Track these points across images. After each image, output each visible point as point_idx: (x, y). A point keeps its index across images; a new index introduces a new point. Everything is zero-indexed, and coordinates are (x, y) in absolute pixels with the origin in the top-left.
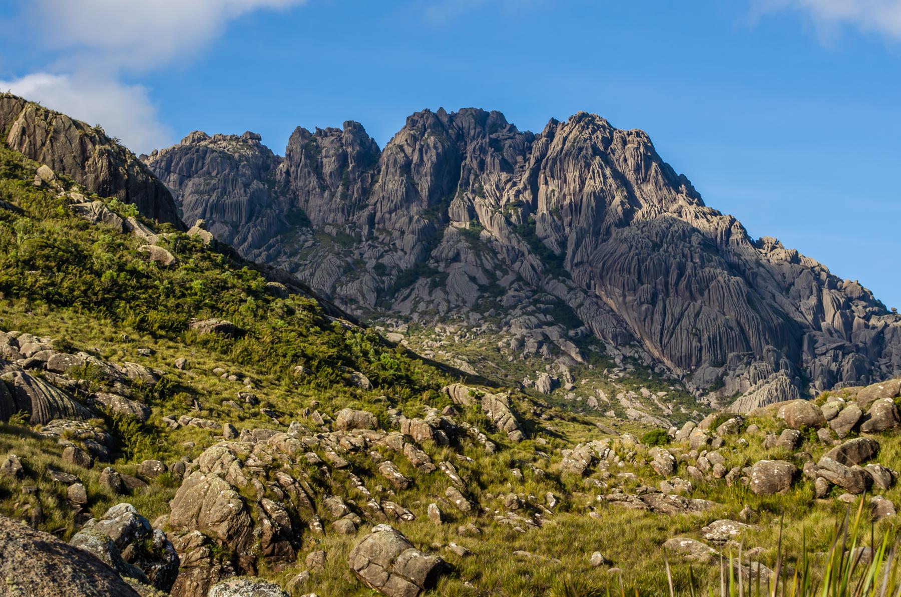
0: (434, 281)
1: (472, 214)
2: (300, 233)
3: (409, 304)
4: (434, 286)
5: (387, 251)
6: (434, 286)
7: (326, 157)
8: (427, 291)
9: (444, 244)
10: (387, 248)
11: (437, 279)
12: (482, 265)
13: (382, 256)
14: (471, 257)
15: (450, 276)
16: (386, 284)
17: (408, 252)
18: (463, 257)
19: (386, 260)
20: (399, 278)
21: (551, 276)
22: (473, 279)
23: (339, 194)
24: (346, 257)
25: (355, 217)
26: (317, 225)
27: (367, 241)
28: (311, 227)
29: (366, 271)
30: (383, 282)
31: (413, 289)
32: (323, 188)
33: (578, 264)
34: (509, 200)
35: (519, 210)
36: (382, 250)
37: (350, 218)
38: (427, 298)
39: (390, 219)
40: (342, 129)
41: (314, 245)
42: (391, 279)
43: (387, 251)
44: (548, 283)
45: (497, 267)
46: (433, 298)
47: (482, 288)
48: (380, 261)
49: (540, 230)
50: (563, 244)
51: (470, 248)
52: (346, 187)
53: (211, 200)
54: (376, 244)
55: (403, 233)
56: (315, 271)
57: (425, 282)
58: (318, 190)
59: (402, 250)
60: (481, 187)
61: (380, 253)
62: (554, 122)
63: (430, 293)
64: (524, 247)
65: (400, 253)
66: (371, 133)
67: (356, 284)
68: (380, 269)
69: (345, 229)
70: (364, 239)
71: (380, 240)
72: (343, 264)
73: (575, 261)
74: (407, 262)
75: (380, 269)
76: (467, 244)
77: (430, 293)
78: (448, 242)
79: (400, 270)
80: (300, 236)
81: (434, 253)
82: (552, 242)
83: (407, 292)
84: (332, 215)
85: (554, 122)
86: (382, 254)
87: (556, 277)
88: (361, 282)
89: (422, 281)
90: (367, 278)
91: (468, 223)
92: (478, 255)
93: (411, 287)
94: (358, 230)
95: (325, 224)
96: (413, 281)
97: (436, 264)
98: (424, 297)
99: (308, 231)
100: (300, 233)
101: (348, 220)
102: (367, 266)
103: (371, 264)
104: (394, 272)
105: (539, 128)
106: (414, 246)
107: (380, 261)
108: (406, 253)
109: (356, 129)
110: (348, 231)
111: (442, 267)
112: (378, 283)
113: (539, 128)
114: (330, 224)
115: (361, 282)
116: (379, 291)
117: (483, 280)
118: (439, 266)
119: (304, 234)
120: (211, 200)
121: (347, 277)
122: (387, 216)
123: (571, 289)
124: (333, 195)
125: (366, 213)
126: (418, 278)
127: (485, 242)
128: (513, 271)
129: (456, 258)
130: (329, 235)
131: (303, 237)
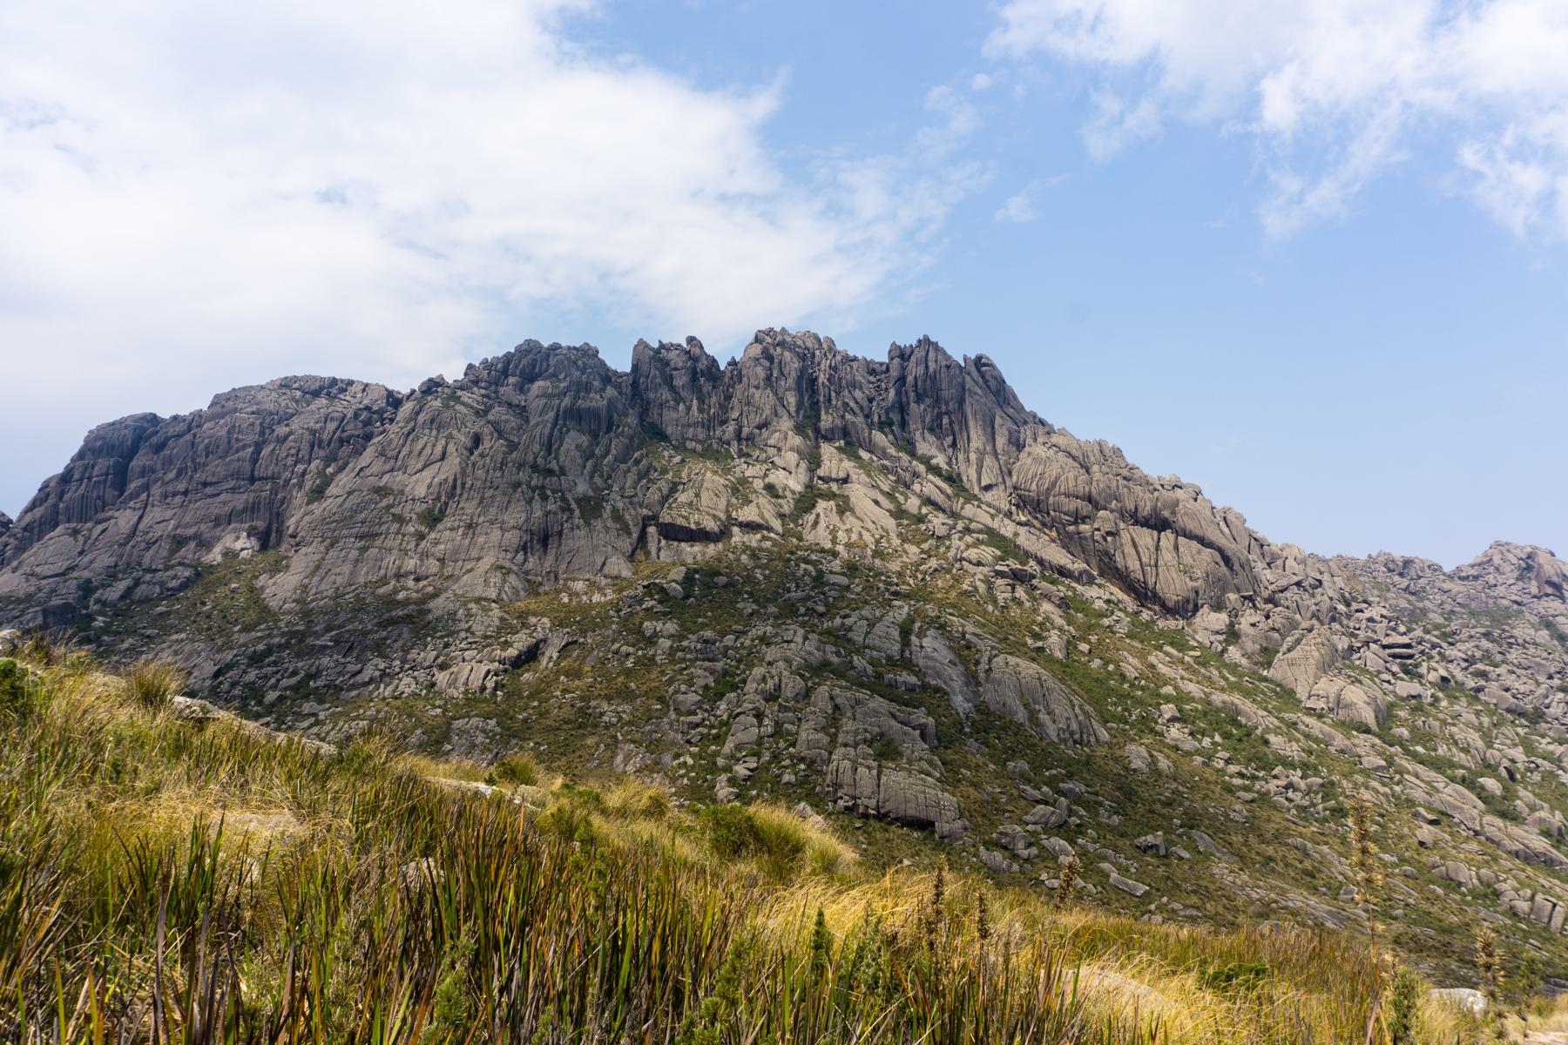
5: (768, 470)
7: (675, 369)
9: (827, 462)
12: (877, 487)
13: (766, 475)
14: (864, 478)
17: (793, 470)
18: (854, 477)
20: (797, 501)
21: (962, 500)
22: (876, 502)
23: (695, 408)
29: (756, 492)
30: (781, 506)
31: (818, 515)
33: (988, 488)
39: (760, 435)
40: (684, 345)
44: (962, 508)
45: (893, 489)
48: (767, 480)
53: (563, 405)
55: (779, 450)
58: (672, 403)
73: (983, 484)
79: (793, 492)
83: (812, 518)
84: (691, 429)
87: (968, 501)
92: (869, 476)
93: (814, 512)
103: (758, 484)
107: (767, 480)
120: (563, 405)
122: (757, 431)
123: (993, 516)
124: (689, 409)
125: (731, 428)
128: (915, 493)
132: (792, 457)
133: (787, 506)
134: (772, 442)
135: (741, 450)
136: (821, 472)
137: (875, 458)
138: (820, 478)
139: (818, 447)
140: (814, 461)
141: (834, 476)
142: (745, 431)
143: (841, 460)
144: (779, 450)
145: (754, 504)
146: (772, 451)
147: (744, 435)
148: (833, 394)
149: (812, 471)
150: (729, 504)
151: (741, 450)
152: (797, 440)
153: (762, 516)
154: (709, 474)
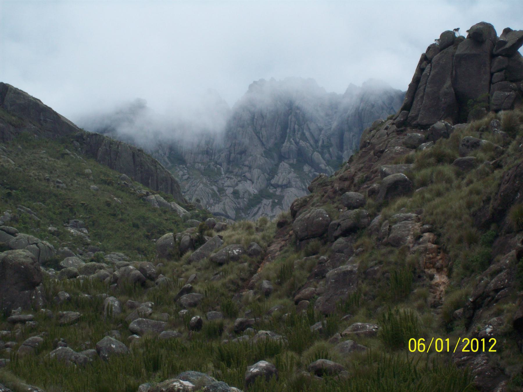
0: (273, 202)
2: (178, 170)
4: (274, 205)
5: (239, 181)
6: (274, 205)
8: (269, 208)
9: (279, 174)
10: (239, 179)
11: (276, 201)
13: (237, 185)
14: (299, 183)
15: (286, 198)
16: (242, 204)
17: (255, 181)
18: (293, 183)
19: (240, 187)
20: (250, 200)
24: (212, 186)
25: (216, 157)
26: (190, 163)
27: (225, 174)
28: (186, 165)
29: (226, 195)
30: (239, 203)
31: (260, 208)
34: (323, 142)
35: (331, 149)
36: (236, 180)
37: (213, 158)
38: (271, 214)
39: (241, 158)
41: (189, 178)
42: (244, 201)
43: (239, 181)
46: (274, 214)
48: (236, 188)
51: (297, 177)
54: (232, 177)
55: (250, 168)
56: (192, 196)
57: (268, 203)
59: (250, 180)
60: (303, 134)
61: (236, 182)
63: (272, 210)
65: (249, 182)
67: (221, 205)
68: (236, 193)
69: (209, 166)
70: (223, 173)
71: (235, 173)
72: (211, 191)
74: (253, 189)
75: (236, 193)
76: (295, 175)
77: (272, 210)
78: (282, 173)
79: (250, 194)
80: (179, 171)
81: (273, 182)
83: (256, 209)
86: (237, 183)
88: (224, 204)
90: (228, 200)
91: (295, 160)
93: (258, 206)
94: (218, 166)
95: (194, 162)
96: (259, 202)
97: (275, 190)
98: (268, 213)
99: (184, 168)
100: (178, 170)
101: (211, 159)
102: (227, 192)
103: (230, 191)
104: (246, 195)
106: (259, 177)
108: (253, 183)
110: (212, 166)
111: (278, 192)
112: (235, 204)
114: (199, 163)
115: (224, 204)
116: (237, 210)
118: (276, 191)
119: (181, 170)
121: (214, 200)
122: (239, 156)
126: (262, 200)
127: (307, 173)
129: (288, 185)
130: (199, 170)
131: (181, 173)
132: (256, 172)
133: (243, 203)
134: (247, 163)
135: (228, 169)
136: (273, 182)
137: (313, 170)
138: (272, 185)
139: (277, 165)
140: (273, 173)
141: (280, 183)
142: (233, 155)
143: (289, 173)
144: (250, 168)
145: (222, 203)
146: (246, 169)
147: (231, 159)
148: (296, 127)
149: (269, 180)
150: (208, 203)
151: (228, 169)
152: (261, 161)
153: (224, 210)
154: (201, 186)
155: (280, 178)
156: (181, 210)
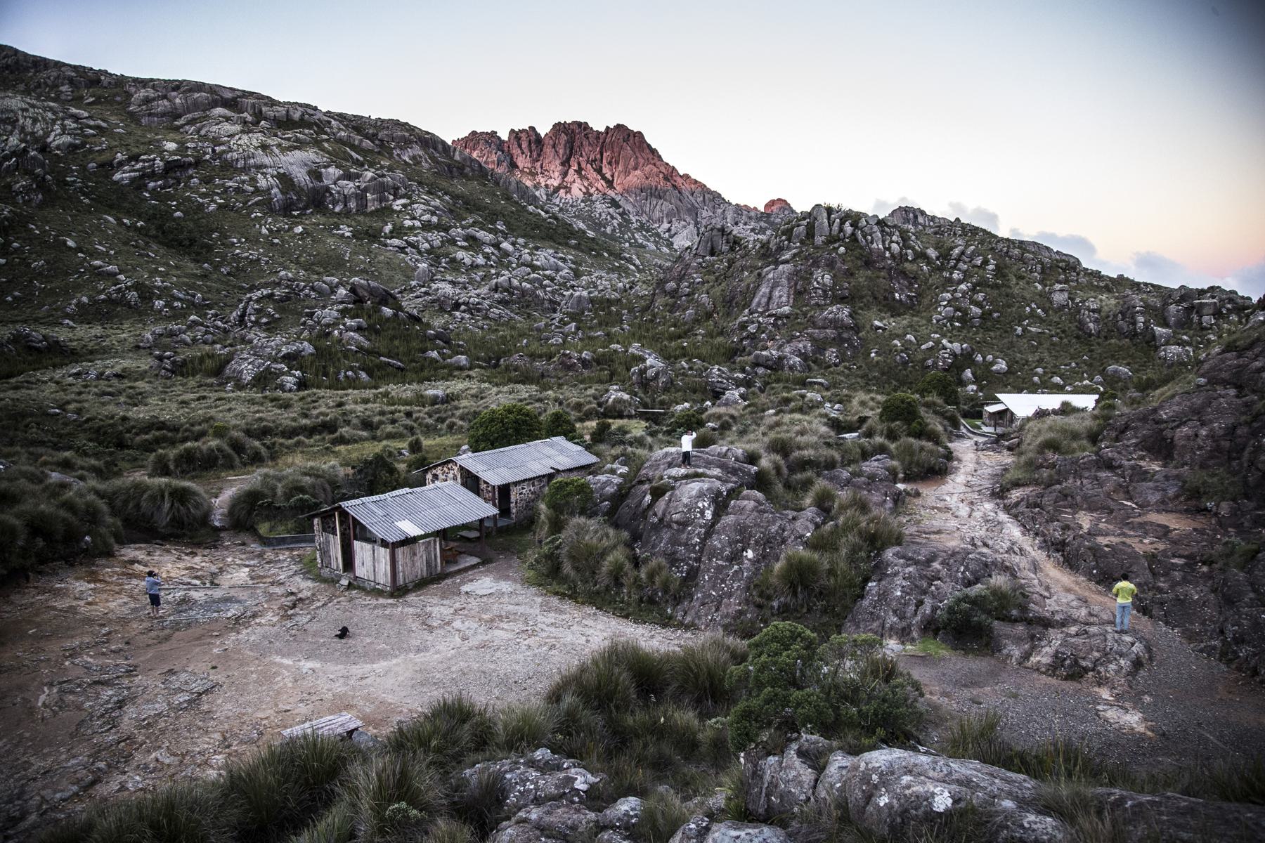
1: (579, 164)
3: (558, 199)
4: (566, 193)
6: (566, 193)
19: (548, 182)
32: (523, 153)
47: (584, 193)
49: (604, 171)
50: (613, 176)
52: (531, 152)
62: (608, 127)
64: (599, 177)
66: (538, 131)
68: (547, 186)
74: (556, 184)
82: (608, 176)
85: (608, 127)
89: (562, 191)
105: (602, 129)
109: (532, 128)
113: (602, 129)
117: (584, 190)
155: (569, 178)
156: (543, 213)
